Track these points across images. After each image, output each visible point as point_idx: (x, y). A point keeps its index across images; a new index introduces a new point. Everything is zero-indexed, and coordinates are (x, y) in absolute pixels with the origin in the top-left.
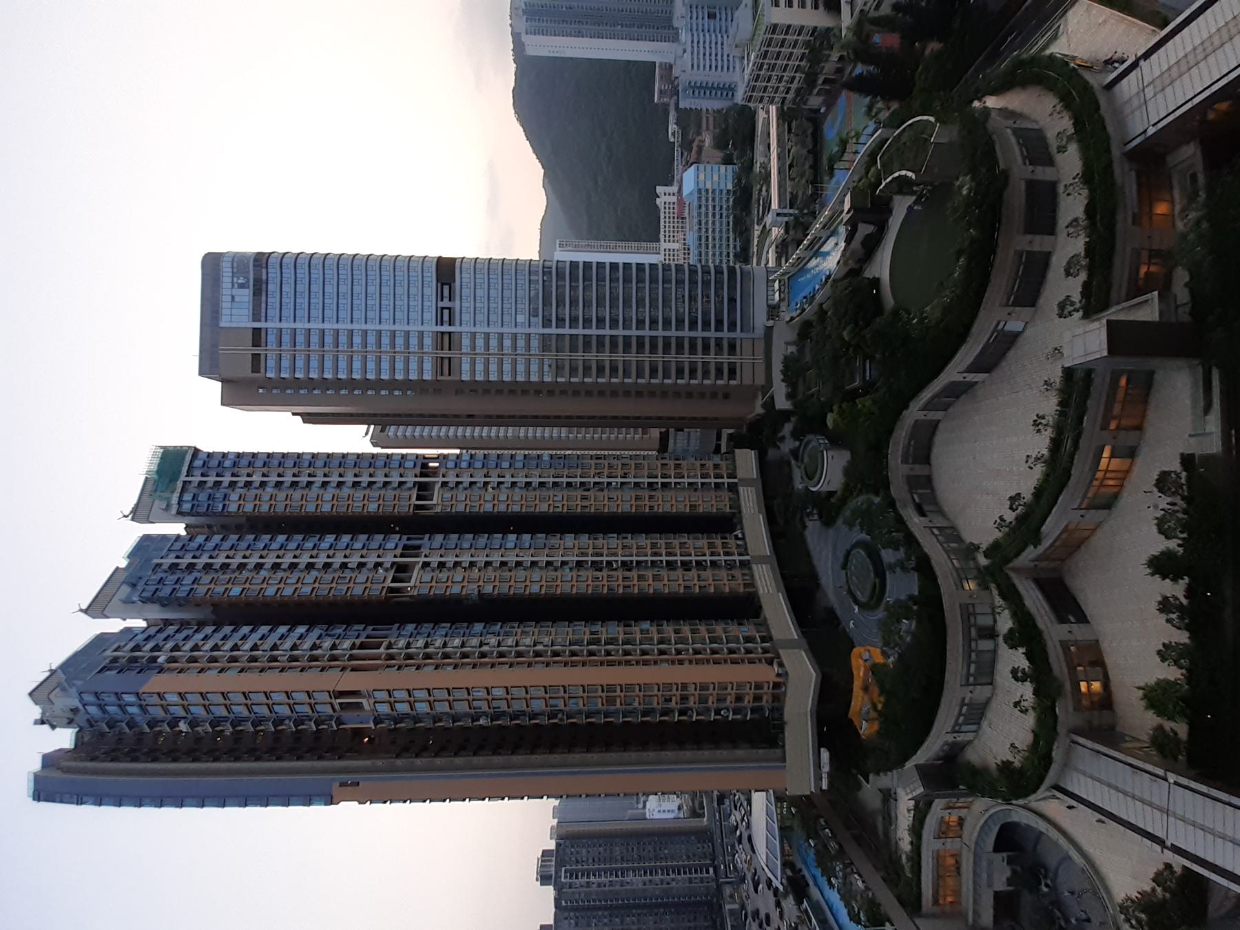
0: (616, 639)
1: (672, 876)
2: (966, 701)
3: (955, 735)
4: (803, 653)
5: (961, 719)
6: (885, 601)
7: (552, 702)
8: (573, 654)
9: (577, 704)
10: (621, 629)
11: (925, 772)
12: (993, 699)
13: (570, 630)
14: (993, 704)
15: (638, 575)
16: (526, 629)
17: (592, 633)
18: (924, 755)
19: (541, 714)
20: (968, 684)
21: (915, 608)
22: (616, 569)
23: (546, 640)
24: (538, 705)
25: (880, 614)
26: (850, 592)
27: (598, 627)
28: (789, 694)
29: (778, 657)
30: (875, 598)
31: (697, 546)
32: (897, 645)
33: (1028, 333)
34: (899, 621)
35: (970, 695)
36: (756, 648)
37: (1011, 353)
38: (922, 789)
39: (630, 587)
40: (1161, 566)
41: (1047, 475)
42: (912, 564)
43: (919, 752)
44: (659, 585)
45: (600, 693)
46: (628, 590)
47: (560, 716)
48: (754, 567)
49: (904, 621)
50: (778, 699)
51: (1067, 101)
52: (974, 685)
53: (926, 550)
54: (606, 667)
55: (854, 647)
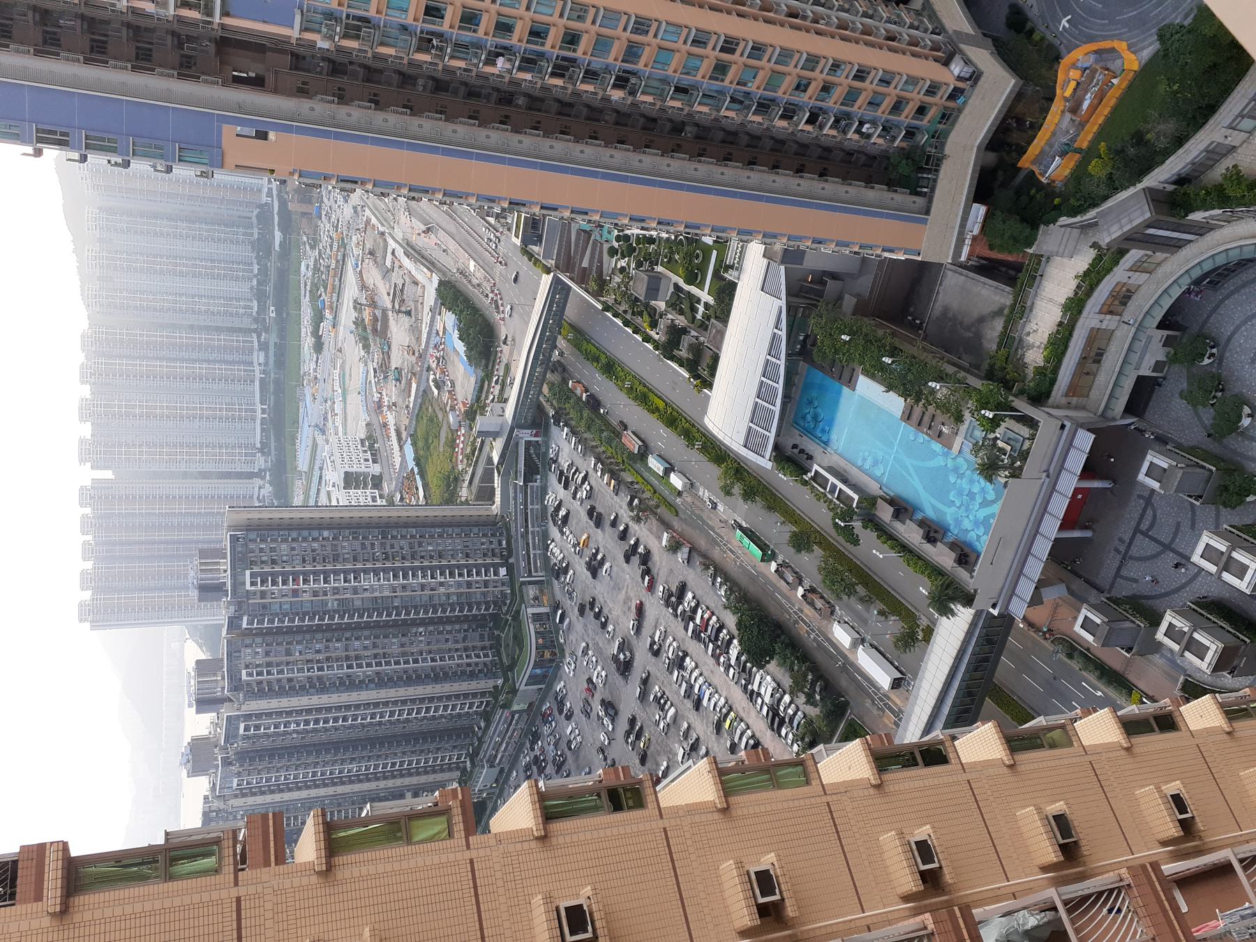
1: (440, 579)
11: (1154, 196)
18: (1160, 177)
38: (1148, 215)
43: (1168, 162)
50: (948, 117)
55: (1057, 58)
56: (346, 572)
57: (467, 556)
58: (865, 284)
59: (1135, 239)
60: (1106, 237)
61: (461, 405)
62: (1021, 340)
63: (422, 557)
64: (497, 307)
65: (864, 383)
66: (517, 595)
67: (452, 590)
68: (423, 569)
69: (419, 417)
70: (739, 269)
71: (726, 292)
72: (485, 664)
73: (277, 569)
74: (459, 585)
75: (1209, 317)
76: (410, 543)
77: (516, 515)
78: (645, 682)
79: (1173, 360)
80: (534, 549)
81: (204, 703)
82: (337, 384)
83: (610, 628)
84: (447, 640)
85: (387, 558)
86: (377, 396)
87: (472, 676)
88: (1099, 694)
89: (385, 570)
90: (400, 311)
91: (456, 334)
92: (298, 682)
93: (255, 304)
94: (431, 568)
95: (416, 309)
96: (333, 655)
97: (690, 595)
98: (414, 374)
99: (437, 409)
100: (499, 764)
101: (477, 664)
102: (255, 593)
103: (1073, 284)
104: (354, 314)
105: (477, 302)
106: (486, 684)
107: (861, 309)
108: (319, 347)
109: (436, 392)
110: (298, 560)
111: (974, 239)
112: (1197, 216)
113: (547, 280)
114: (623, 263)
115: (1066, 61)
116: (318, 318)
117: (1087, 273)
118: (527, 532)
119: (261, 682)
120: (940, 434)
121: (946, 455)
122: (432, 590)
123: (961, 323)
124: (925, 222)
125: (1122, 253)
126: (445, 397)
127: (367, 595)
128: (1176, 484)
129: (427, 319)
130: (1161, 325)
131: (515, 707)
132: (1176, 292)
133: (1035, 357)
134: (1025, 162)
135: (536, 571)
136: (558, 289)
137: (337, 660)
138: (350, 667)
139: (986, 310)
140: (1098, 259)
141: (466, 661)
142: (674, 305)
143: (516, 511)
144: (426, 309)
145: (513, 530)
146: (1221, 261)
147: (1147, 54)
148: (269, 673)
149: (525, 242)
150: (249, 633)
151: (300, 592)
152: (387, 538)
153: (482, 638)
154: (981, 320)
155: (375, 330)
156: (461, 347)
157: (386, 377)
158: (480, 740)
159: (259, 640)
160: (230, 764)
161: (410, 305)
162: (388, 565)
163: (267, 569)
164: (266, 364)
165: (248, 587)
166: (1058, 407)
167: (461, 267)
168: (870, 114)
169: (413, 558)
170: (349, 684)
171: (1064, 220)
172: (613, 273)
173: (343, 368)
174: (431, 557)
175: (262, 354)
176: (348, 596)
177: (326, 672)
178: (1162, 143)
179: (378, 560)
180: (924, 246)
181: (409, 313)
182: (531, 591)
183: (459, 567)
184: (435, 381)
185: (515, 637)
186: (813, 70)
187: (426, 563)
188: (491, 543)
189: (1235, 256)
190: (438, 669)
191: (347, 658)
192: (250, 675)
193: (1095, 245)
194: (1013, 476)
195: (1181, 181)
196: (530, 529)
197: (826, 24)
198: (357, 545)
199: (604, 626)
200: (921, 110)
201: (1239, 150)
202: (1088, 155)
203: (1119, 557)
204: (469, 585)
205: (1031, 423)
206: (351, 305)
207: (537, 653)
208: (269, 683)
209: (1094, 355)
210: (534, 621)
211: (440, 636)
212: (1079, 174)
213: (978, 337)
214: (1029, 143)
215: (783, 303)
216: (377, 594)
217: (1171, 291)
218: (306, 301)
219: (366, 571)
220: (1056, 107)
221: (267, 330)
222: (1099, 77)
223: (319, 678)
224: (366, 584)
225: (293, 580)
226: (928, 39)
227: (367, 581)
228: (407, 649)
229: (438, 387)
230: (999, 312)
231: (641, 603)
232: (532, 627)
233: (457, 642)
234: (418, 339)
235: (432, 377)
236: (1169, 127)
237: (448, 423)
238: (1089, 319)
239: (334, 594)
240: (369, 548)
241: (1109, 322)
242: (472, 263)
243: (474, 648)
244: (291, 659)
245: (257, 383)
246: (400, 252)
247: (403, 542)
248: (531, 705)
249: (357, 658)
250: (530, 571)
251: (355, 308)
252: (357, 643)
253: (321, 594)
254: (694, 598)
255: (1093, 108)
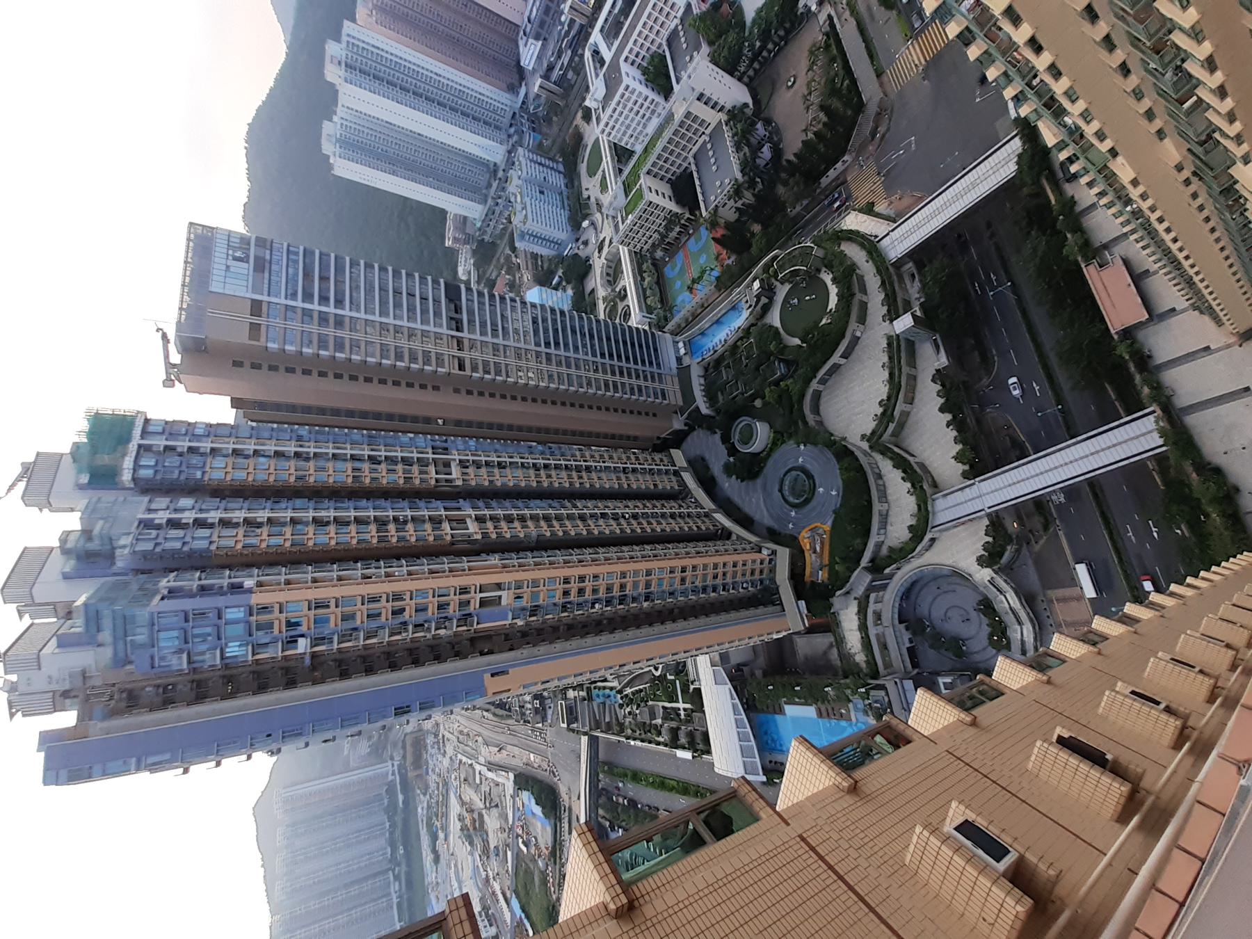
31: (671, 507)
33: (864, 336)
37: (857, 347)
40: (942, 410)
41: (890, 389)
50: (772, 570)
51: (862, 246)
58: (762, 661)
59: (870, 589)
60: (860, 591)
61: (545, 851)
64: (554, 774)
65: (788, 709)
69: (516, 874)
70: (699, 680)
71: (696, 697)
79: (914, 634)
82: (453, 879)
86: (484, 874)
90: (491, 807)
91: (533, 801)
93: (389, 850)
95: (501, 802)
98: (508, 845)
99: (528, 862)
103: (856, 618)
104: (459, 825)
105: (539, 777)
107: (765, 674)
108: (437, 860)
109: (524, 849)
112: (887, 571)
113: (584, 739)
114: (628, 709)
115: (800, 538)
116: (434, 838)
117: (859, 611)
120: (841, 715)
121: (851, 725)
126: (533, 850)
129: (509, 803)
132: (897, 605)
133: (860, 658)
134: (807, 578)
136: (594, 741)
139: (824, 647)
140: (859, 604)
142: (665, 718)
144: (508, 797)
146: (903, 589)
147: (830, 523)
149: (568, 725)
155: (475, 828)
156: (538, 810)
157: (488, 857)
161: (497, 800)
164: (400, 890)
167: (525, 760)
168: (744, 580)
171: (838, 593)
172: (625, 717)
173: (456, 866)
175: (397, 884)
178: (861, 547)
181: (497, 806)
184: (523, 842)
189: (910, 581)
193: (855, 599)
195: (872, 561)
200: (761, 572)
202: (831, 566)
205: (883, 687)
206: (456, 819)
209: (884, 647)
212: (832, 572)
213: (829, 661)
215: (730, 685)
218: (424, 832)
220: (807, 555)
221: (399, 865)
222: (817, 537)
226: (748, 547)
229: (526, 845)
230: (831, 646)
234: (506, 819)
235: (520, 841)
236: (858, 541)
237: (539, 868)
238: (873, 632)
242: (532, 755)
245: (395, 907)
246: (484, 770)
251: (459, 820)
255: (822, 548)
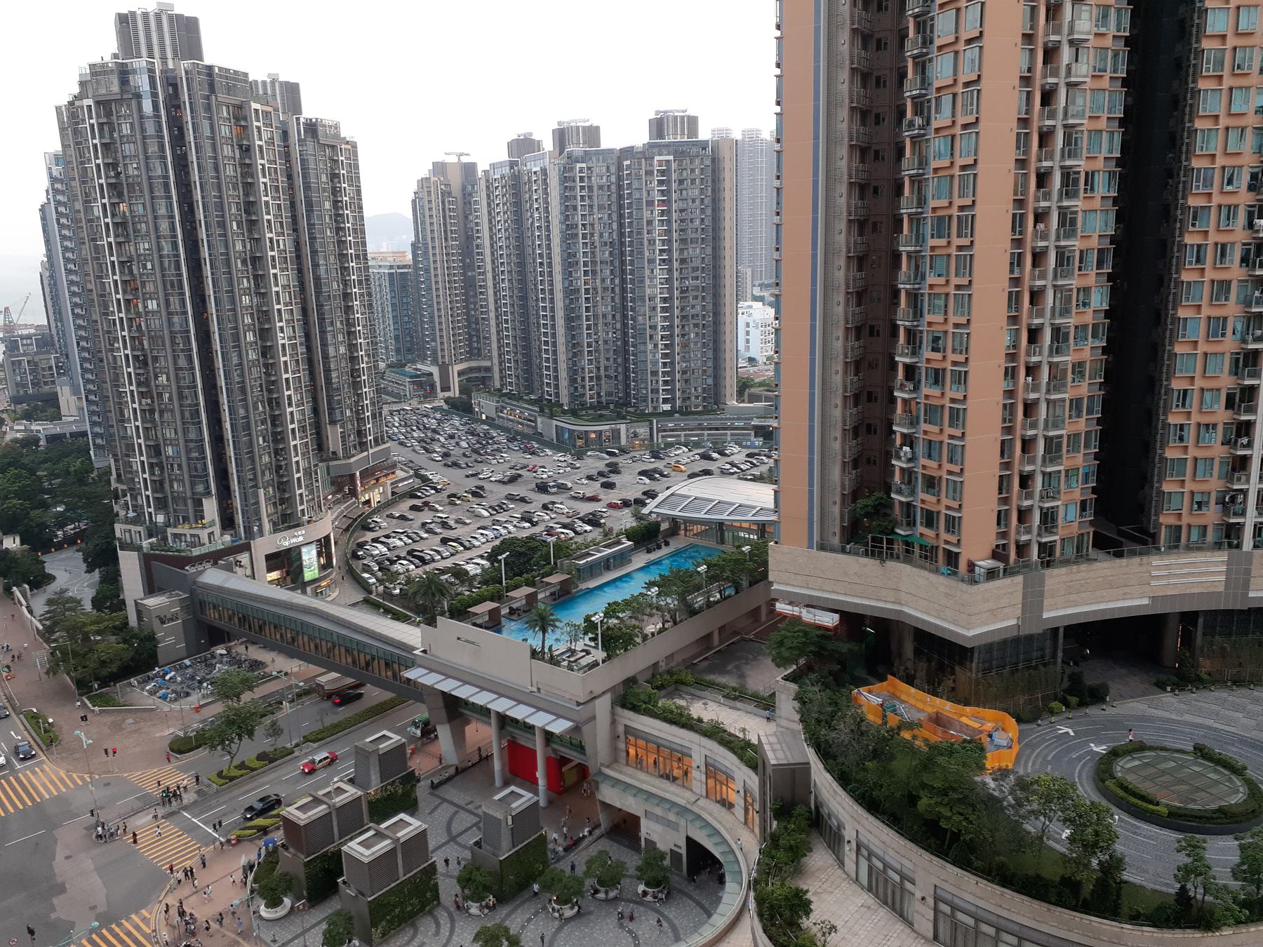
0: (1071, 234)
2: (908, 885)
3: (854, 844)
4: (1013, 622)
5: (880, 865)
6: (1114, 809)
7: (947, 100)
8: (1045, 137)
9: (939, 156)
10: (1094, 243)
12: (908, 931)
13: (1103, 124)
14: (899, 926)
15: (1229, 282)
16: (1113, 14)
17: (1090, 176)
18: (823, 781)
19: (923, 81)
20: (937, 899)
21: (1095, 862)
22: (1251, 225)
23: (1083, 71)
24: (941, 70)
25: (1086, 792)
26: (1141, 747)
27: (1104, 188)
28: (933, 577)
29: (1008, 572)
30: (1121, 793)
32: (1019, 804)
34: (1067, 821)
35: (918, 895)
36: (1029, 531)
38: (773, 762)
39: (1198, 261)
42: (1196, 891)
44: (1198, 331)
45: (958, 202)
46: (1190, 257)
47: (918, 121)
48: (1222, 556)
49: (1067, 833)
52: (936, 910)
53: (1227, 932)
54: (1011, 212)
55: (1019, 720)
56: (669, 251)
57: (684, 372)
62: (701, 698)
63: (683, 326)
66: (642, 417)
67: (650, 357)
68: (671, 327)
72: (584, 395)
73: (674, 186)
74: (655, 363)
75: (691, 898)
76: (697, 316)
77: (722, 419)
78: (523, 500)
80: (685, 435)
81: (561, 136)
83: (585, 481)
84: (608, 359)
85: (682, 292)
87: (572, 381)
88: (335, 779)
89: (670, 290)
92: (573, 215)
94: (672, 336)
96: (598, 249)
97: (588, 528)
100: (499, 416)
101: (583, 387)
102: (651, 165)
106: (565, 400)
110: (682, 205)
111: (799, 618)
118: (703, 429)
119: (574, 181)
122: (651, 337)
123: (747, 663)
124: (810, 547)
125: (754, 767)
127: (647, 272)
128: (490, 812)
130: (691, 843)
131: (539, 420)
135: (663, 437)
137: (593, 253)
138: (585, 264)
141: (587, 376)
143: (726, 419)
145: (704, 417)
148: (582, 188)
150: (620, 168)
151: (651, 208)
152: (703, 291)
153: (609, 394)
154: (742, 676)
158: (521, 398)
159: (613, 179)
160: (512, 168)
162: (676, 293)
163: (674, 176)
165: (657, 158)
166: (614, 722)
169: (683, 317)
170: (570, 263)
174: (683, 336)
176: (647, 254)
177: (581, 241)
179: (681, 283)
180: (784, 548)
182: (643, 430)
183: (672, 363)
185: (601, 416)
186: (954, 351)
187: (677, 331)
188: (697, 397)
190: (579, 349)
191: (594, 263)
192: (581, 171)
194: (534, 654)
196: (706, 432)
197: (1026, 384)
198: (697, 263)
199: (590, 478)
201: (840, 872)
203: (462, 803)
204: (655, 373)
207: (581, 432)
208: (572, 189)
210: (613, 430)
211: (612, 352)
213: (728, 672)
214: (917, 687)
216: (647, 282)
217: (723, 848)
219: (670, 271)
223: (577, 235)
224: (656, 271)
225: (663, 201)
227: (660, 274)
228: (601, 321)
231: (600, 500)
232: (607, 427)
233: (606, 368)
239: (649, 241)
240: (694, 275)
241: (698, 776)
243: (599, 385)
244: (595, 210)
247: (698, 308)
248: (541, 434)
249: (594, 272)
250: (665, 431)
252: (608, 272)
253: (649, 228)
254: (586, 531)
